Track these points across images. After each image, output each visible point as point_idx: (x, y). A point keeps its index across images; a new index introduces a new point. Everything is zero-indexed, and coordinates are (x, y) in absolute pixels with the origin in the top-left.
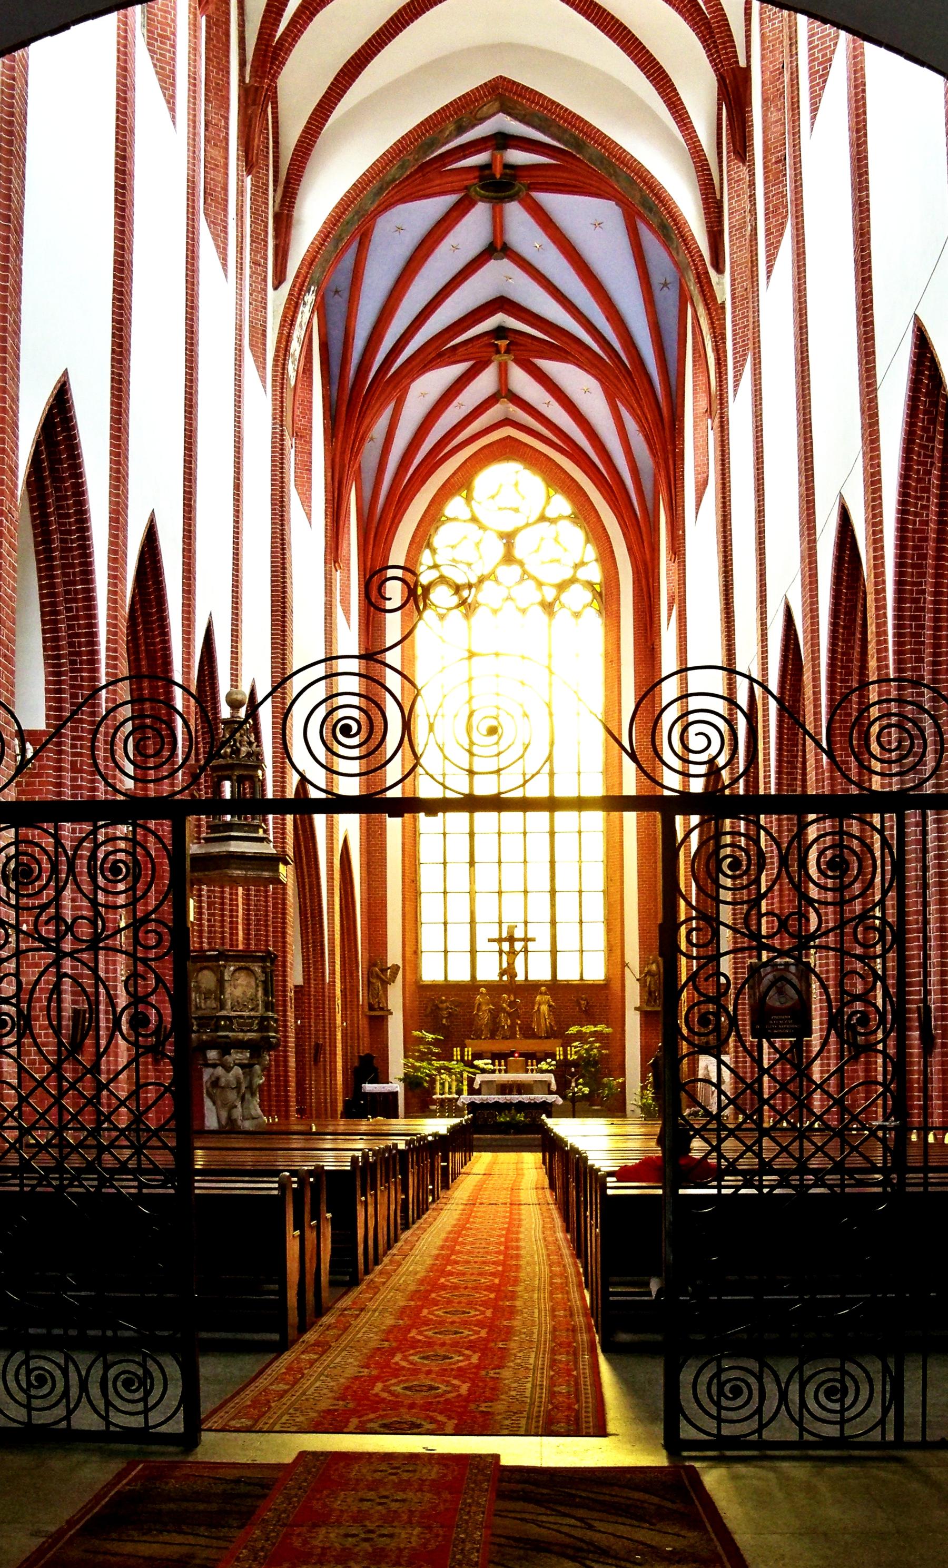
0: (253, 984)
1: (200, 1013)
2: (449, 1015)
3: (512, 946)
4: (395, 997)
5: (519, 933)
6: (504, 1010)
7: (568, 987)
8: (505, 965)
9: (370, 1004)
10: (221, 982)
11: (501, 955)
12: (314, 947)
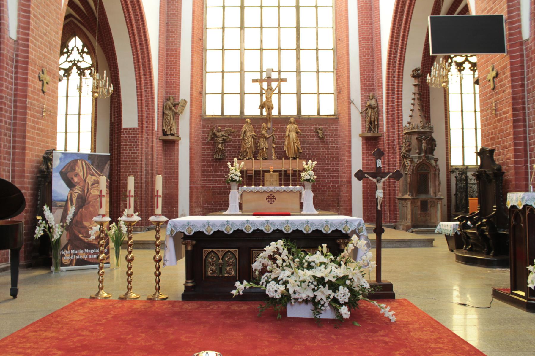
2: (222, 140)
3: (269, 85)
4: (184, 129)
6: (263, 136)
7: (309, 120)
8: (264, 99)
11: (261, 96)
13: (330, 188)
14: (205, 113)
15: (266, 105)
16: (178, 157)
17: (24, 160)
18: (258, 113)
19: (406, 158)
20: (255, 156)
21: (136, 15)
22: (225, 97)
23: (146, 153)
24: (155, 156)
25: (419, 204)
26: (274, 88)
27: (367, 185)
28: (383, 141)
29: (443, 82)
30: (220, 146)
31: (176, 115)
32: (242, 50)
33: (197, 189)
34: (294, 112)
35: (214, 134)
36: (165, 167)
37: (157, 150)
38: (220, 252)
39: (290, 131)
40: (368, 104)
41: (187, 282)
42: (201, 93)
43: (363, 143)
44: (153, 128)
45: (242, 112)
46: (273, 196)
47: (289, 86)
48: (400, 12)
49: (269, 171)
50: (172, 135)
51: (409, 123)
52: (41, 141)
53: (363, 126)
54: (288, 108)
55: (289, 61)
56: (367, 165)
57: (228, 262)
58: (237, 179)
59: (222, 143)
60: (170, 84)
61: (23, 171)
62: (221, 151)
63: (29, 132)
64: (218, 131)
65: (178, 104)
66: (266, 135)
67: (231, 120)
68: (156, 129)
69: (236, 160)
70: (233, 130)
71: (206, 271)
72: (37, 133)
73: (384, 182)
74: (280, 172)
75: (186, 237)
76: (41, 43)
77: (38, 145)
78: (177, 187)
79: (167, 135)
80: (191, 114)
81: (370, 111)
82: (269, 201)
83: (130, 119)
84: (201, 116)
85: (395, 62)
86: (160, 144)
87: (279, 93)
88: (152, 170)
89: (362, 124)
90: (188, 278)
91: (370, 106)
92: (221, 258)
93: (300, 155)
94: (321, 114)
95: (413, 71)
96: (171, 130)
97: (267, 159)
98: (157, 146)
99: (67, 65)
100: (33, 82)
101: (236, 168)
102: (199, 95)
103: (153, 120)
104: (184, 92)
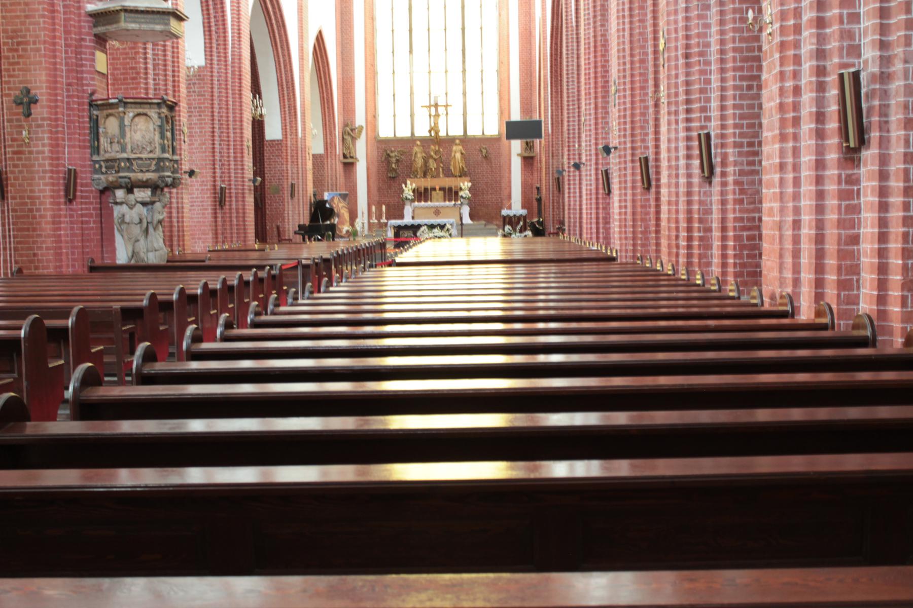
0: (151, 128)
1: (107, 156)
3: (437, 110)
5: (441, 102)
6: (432, 157)
10: (122, 127)
12: (290, 110)
15: (434, 129)
20: (425, 176)
21: (323, 62)
31: (354, 139)
34: (460, 133)
35: (388, 155)
45: (412, 133)
49: (434, 189)
50: (352, 157)
58: (410, 197)
64: (392, 152)
66: (435, 156)
69: (408, 182)
84: (375, 138)
93: (463, 174)
98: (340, 168)
101: (408, 190)
104: (360, 119)
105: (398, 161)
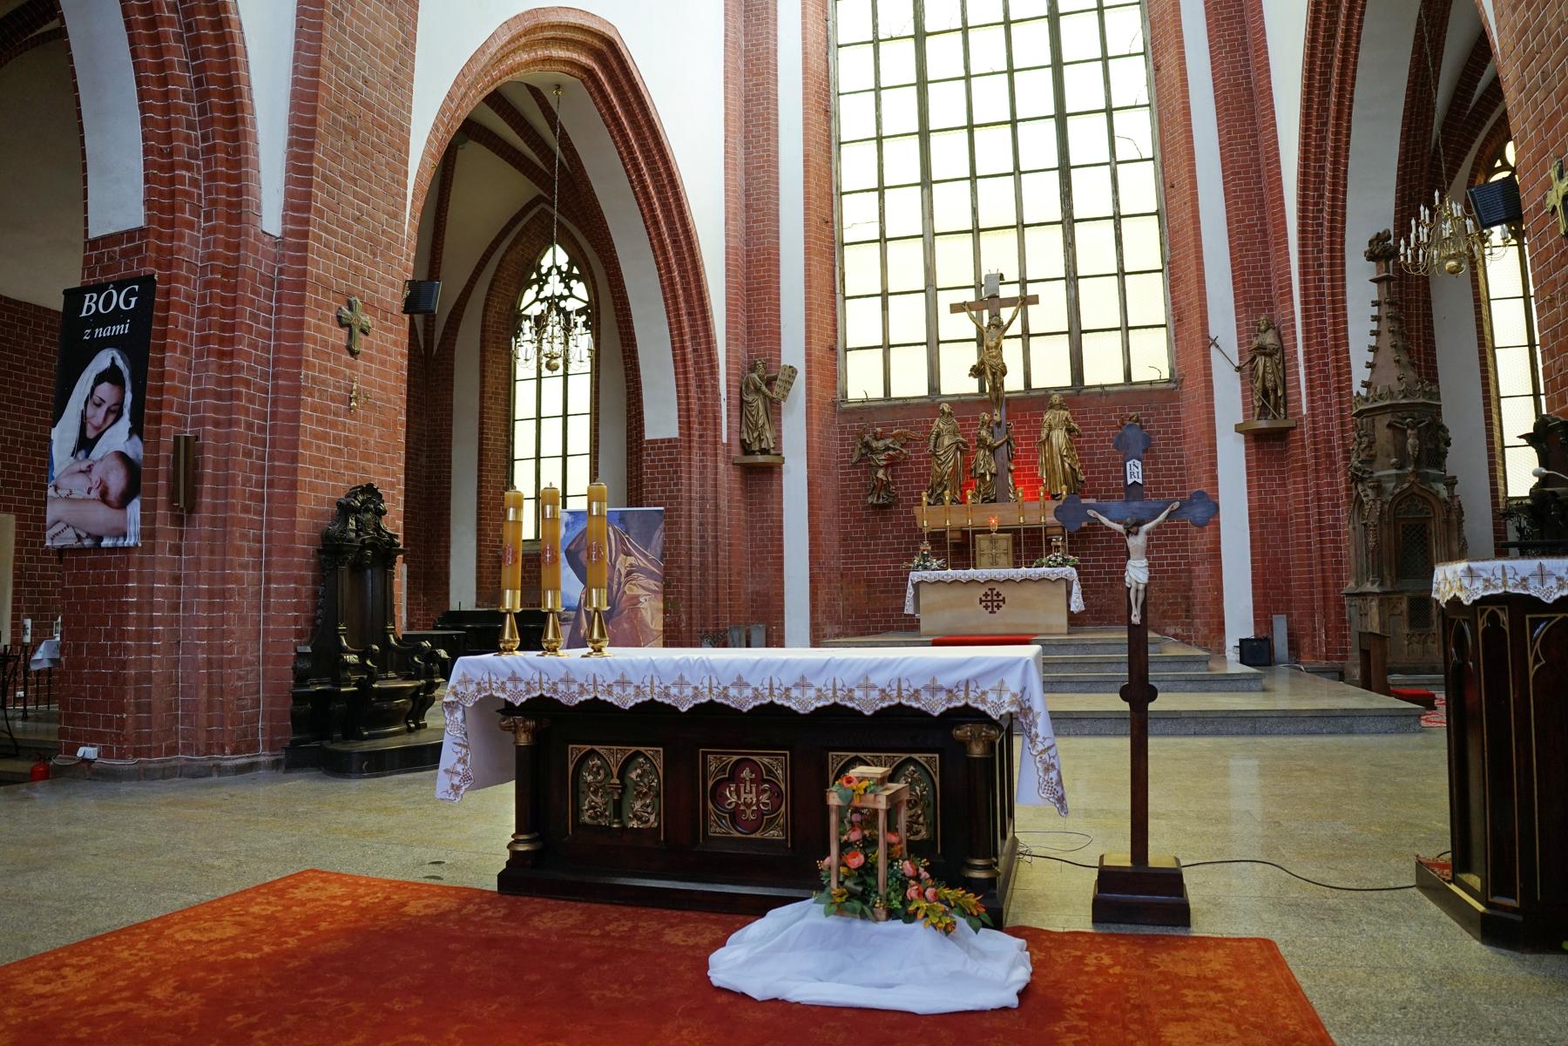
6: (982, 443)
9: (743, 441)
13: (1166, 571)
14: (845, 394)
15: (988, 369)
16: (781, 503)
17: (293, 513)
18: (972, 386)
19: (1362, 480)
21: (655, 175)
22: (894, 352)
23: (702, 498)
24: (723, 504)
25: (1404, 606)
26: (1005, 322)
27: (1263, 561)
28: (1303, 440)
29: (1450, 258)
30: (880, 474)
31: (774, 408)
32: (929, 237)
33: (830, 581)
35: (867, 445)
36: (752, 528)
37: (729, 489)
38: (614, 755)
39: (1051, 428)
40: (1256, 342)
41: (517, 842)
42: (833, 349)
43: (1247, 448)
44: (717, 436)
45: (934, 386)
46: (998, 595)
47: (1049, 312)
48: (1320, 88)
50: (764, 452)
51: (1366, 385)
52: (346, 468)
53: (1245, 404)
54: (1051, 372)
55: (1046, 253)
56: (1260, 507)
57: (636, 784)
59: (886, 466)
60: (756, 333)
61: (292, 538)
62: (885, 486)
63: (308, 446)
65: (775, 379)
67: (907, 405)
68: (725, 440)
70: (913, 434)
71: (577, 811)
72: (333, 449)
73: (1148, 533)
74: (1015, 532)
75: (508, 709)
76: (345, 239)
77: (336, 476)
78: (782, 577)
79: (753, 453)
80: (809, 401)
81: (1261, 361)
82: (986, 607)
83: (661, 422)
84: (834, 404)
85: (1321, 225)
86: (735, 474)
87: (1026, 335)
88: (716, 537)
89: (1244, 397)
90: (520, 828)
91: (1262, 350)
92: (615, 771)
94: (1134, 379)
95: (1371, 242)
96: (761, 441)
97: (995, 501)
98: (727, 478)
99: (536, 309)
100: (318, 329)
102: (829, 353)
103: (716, 418)
104: (793, 351)
105: (892, 463)
